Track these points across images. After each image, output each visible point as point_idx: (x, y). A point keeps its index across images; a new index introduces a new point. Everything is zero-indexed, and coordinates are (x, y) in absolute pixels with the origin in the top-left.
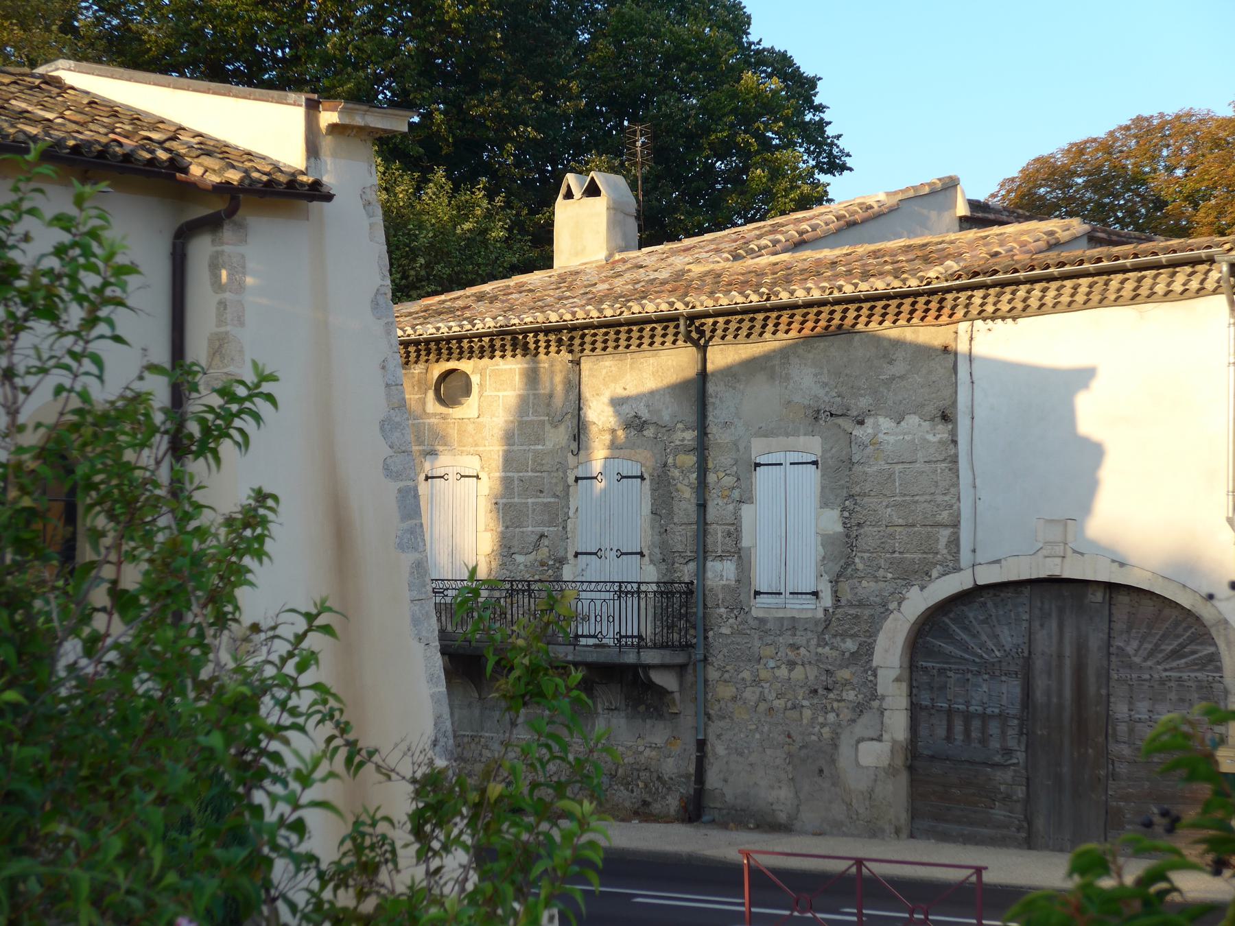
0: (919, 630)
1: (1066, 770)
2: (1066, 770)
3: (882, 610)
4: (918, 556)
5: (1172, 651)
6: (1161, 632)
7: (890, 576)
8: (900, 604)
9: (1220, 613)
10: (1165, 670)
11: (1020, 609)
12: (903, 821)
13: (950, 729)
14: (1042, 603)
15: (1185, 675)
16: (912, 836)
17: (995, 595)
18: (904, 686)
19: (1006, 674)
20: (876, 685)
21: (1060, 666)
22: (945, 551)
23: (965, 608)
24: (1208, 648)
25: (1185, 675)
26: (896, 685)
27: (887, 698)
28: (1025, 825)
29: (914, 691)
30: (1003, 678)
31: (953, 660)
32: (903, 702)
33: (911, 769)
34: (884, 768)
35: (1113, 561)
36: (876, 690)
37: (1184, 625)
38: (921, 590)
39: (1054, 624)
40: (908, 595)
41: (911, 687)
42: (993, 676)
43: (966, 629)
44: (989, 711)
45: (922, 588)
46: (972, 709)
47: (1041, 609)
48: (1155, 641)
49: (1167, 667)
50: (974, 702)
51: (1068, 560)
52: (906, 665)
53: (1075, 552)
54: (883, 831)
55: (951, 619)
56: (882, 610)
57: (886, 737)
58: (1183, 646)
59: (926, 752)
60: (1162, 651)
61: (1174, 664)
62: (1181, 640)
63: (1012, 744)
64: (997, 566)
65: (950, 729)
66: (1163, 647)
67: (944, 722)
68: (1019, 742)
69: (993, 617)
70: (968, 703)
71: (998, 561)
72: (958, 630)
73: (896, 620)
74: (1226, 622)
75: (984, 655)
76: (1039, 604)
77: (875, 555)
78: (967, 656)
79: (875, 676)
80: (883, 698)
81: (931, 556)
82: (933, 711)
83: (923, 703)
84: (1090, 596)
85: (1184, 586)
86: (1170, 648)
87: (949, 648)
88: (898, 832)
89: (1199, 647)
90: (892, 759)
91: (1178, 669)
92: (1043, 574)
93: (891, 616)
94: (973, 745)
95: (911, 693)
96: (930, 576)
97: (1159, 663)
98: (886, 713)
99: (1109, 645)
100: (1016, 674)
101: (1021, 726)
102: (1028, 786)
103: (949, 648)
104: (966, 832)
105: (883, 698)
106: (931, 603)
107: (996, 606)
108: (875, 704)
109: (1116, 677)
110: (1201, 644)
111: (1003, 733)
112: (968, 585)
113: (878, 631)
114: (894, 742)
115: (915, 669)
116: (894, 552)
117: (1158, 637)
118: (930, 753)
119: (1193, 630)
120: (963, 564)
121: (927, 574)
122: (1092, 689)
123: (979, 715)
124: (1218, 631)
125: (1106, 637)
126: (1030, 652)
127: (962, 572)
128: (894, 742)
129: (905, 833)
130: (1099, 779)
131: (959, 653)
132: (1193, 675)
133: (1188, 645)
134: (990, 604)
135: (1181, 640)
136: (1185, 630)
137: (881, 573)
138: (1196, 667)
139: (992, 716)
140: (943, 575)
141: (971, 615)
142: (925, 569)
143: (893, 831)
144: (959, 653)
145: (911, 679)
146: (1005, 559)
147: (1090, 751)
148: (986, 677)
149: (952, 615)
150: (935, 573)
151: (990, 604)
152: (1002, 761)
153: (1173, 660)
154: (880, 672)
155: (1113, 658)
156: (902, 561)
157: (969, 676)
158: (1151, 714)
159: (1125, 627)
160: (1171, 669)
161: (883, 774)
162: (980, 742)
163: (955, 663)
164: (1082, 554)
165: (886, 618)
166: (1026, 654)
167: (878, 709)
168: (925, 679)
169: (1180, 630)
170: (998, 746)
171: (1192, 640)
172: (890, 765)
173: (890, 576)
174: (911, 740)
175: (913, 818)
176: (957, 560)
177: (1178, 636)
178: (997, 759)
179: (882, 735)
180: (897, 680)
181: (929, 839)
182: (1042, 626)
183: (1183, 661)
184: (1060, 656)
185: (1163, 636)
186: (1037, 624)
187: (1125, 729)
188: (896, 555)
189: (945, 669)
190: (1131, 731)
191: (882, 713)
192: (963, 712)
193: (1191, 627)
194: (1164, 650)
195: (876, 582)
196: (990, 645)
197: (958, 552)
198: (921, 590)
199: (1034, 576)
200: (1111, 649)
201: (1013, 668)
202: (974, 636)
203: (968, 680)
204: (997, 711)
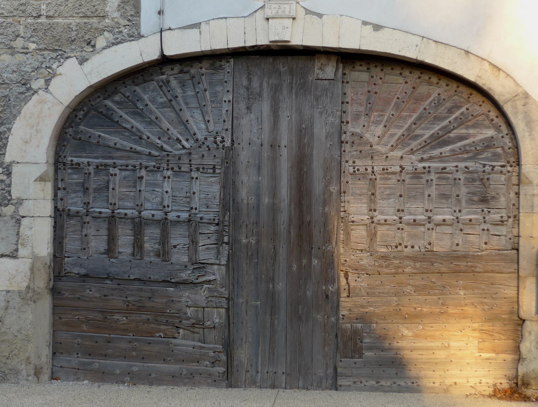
0: (68, 117)
1: (281, 286)
2: (281, 286)
3: (23, 89)
4: (74, 21)
5: (432, 136)
6: (415, 116)
7: (33, 46)
8: (47, 82)
9: (517, 84)
10: (422, 160)
11: (219, 89)
12: (44, 359)
13: (112, 240)
14: (250, 80)
15: (450, 166)
16: (53, 377)
17: (181, 72)
18: (49, 187)
19: (198, 170)
20: (9, 185)
21: (274, 160)
22: (116, 14)
23: (137, 89)
24: (484, 131)
25: (450, 166)
26: (39, 186)
27: (26, 203)
28: (223, 358)
29: (60, 194)
30: (194, 174)
31: (119, 154)
32: (48, 208)
33: (54, 292)
34: (20, 292)
35: (365, 23)
36: (9, 192)
37: (449, 105)
38: (81, 63)
39: (266, 107)
40: (60, 70)
41: (56, 189)
42: (178, 173)
43: (139, 114)
44: (172, 216)
45: (82, 61)
46: (146, 214)
47: (247, 88)
48: (407, 126)
49: (425, 156)
50: (147, 205)
51: (299, 22)
52: (51, 161)
53: (308, 12)
54: (17, 373)
55: (117, 103)
56: (23, 89)
57: (22, 252)
58: (447, 130)
59: (76, 270)
60: (416, 137)
61: (436, 152)
62: (446, 122)
63: (204, 255)
64: (196, 31)
65: (112, 240)
66: (418, 132)
67: (104, 232)
68: (218, 253)
69: (180, 99)
70: (139, 208)
71: (197, 26)
72: (125, 116)
73: (42, 102)
74: (526, 96)
75: (165, 146)
76: (245, 82)
77: (10, 20)
78: (139, 148)
79: (9, 174)
80: (20, 202)
81: (95, 20)
82: (88, 219)
83: (73, 209)
84: (317, 71)
85: (467, 52)
86: (428, 134)
87: (113, 139)
88: (37, 373)
89: (471, 131)
90: (32, 279)
91: (441, 158)
92: (263, 41)
93: (35, 97)
94: (147, 259)
95: (56, 195)
96: (94, 46)
97: (412, 152)
98: (24, 222)
99: (341, 132)
100: (214, 168)
101: (220, 234)
102: (228, 309)
103: (113, 139)
104: (135, 369)
105: (20, 202)
106: (95, 79)
107: (183, 85)
108: (9, 210)
109: (351, 170)
110: (474, 126)
111: (194, 242)
112: (153, 55)
113: (15, 116)
114: (35, 258)
115: (61, 166)
116: (39, 16)
117: (410, 121)
118: (83, 271)
119: (463, 109)
120: (144, 30)
121: (89, 44)
122: (318, 187)
123: (158, 221)
124: (515, 107)
125: (338, 121)
126: (233, 141)
127: (142, 40)
128: (35, 258)
129: (45, 376)
130: (327, 296)
131: (128, 145)
132: (462, 165)
133: (454, 128)
134: (174, 83)
135: (446, 122)
136: (450, 111)
137: (19, 43)
138: (466, 156)
139: (177, 222)
140: (114, 44)
141: (146, 97)
142: (87, 37)
143: (32, 372)
144: (128, 145)
145: (56, 180)
146: (207, 22)
147: (315, 262)
148: (169, 173)
149: (117, 98)
150: (101, 42)
151: (174, 83)
152: (192, 278)
153: (434, 148)
154: (15, 169)
155: (347, 147)
156: (51, 27)
157: (143, 173)
158: (429, 214)
159: (362, 109)
160: (431, 159)
161: (18, 299)
162: (158, 255)
163: (121, 158)
164: (320, 16)
165: (26, 100)
166: (228, 143)
167: (12, 217)
168: (76, 178)
169: (442, 110)
170: (185, 259)
171: (461, 122)
172: (28, 287)
173: (33, 46)
174: (54, 256)
175: (54, 354)
176: (137, 26)
177: (438, 119)
178: (184, 275)
179: (17, 250)
180: (41, 179)
181: (78, 379)
182: (249, 108)
183: (449, 148)
184: (274, 146)
185: (419, 118)
186: (242, 106)
187: (365, 233)
188: (43, 20)
189: (106, 165)
190: (372, 236)
191: (18, 222)
192: (133, 219)
193: (459, 107)
194: (421, 136)
195: (12, 54)
196: (175, 132)
197: (138, 13)
198: (81, 63)
199: (250, 43)
200: (343, 137)
201: (209, 161)
202: (150, 123)
203: (142, 178)
204: (184, 216)
